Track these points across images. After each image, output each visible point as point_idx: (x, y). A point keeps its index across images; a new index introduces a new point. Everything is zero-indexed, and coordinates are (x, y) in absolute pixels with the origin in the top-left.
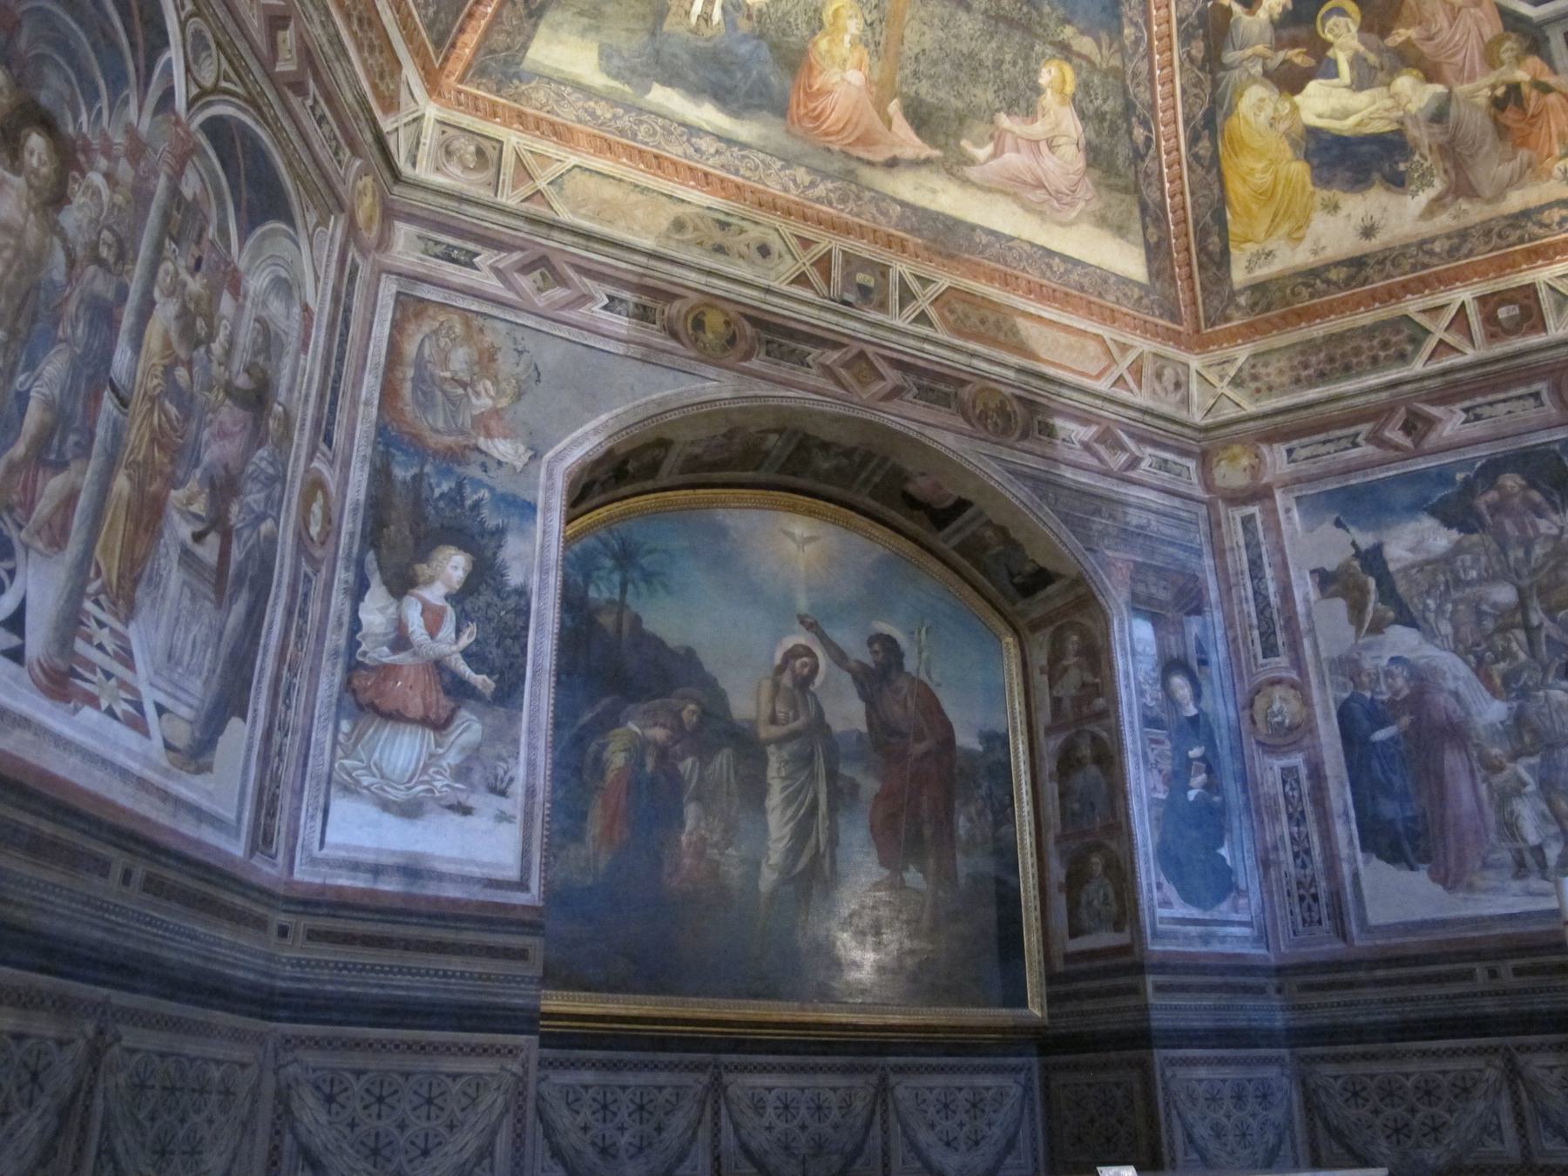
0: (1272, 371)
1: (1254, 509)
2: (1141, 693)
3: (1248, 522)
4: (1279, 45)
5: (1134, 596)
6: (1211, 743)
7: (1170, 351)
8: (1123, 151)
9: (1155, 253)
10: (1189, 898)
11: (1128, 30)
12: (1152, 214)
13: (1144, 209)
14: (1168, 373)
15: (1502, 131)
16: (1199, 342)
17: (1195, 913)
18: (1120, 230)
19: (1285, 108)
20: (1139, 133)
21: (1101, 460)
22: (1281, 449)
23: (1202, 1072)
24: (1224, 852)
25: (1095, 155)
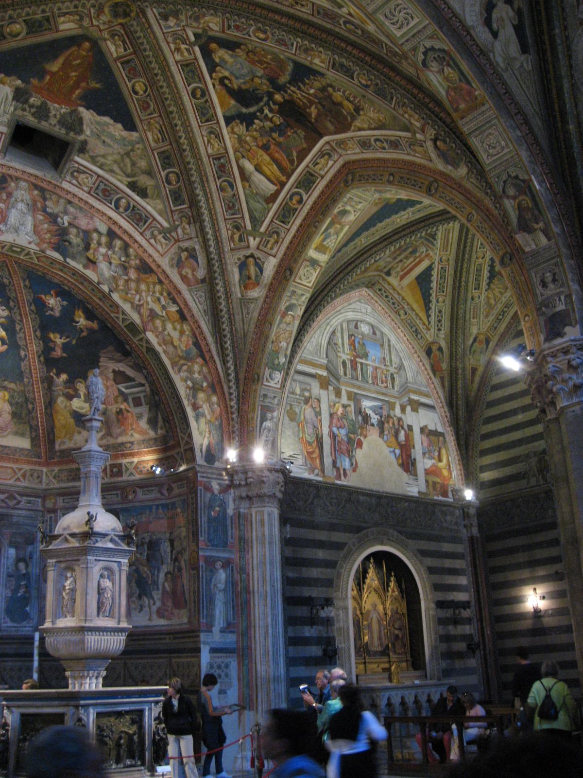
0: (63, 476)
1: (53, 515)
2: (8, 568)
3: (51, 518)
4: (66, 388)
5: (11, 542)
6: (29, 580)
7: (37, 468)
8: (25, 412)
9: (34, 441)
10: (12, 620)
11: (26, 380)
12: (33, 429)
13: (31, 427)
14: (35, 474)
15: (118, 420)
16: (47, 464)
17: (15, 625)
18: (22, 435)
19: (68, 404)
20: (30, 406)
21: (6, 503)
22: (61, 499)
23: (10, 664)
24: (28, 609)
25: (14, 415)
